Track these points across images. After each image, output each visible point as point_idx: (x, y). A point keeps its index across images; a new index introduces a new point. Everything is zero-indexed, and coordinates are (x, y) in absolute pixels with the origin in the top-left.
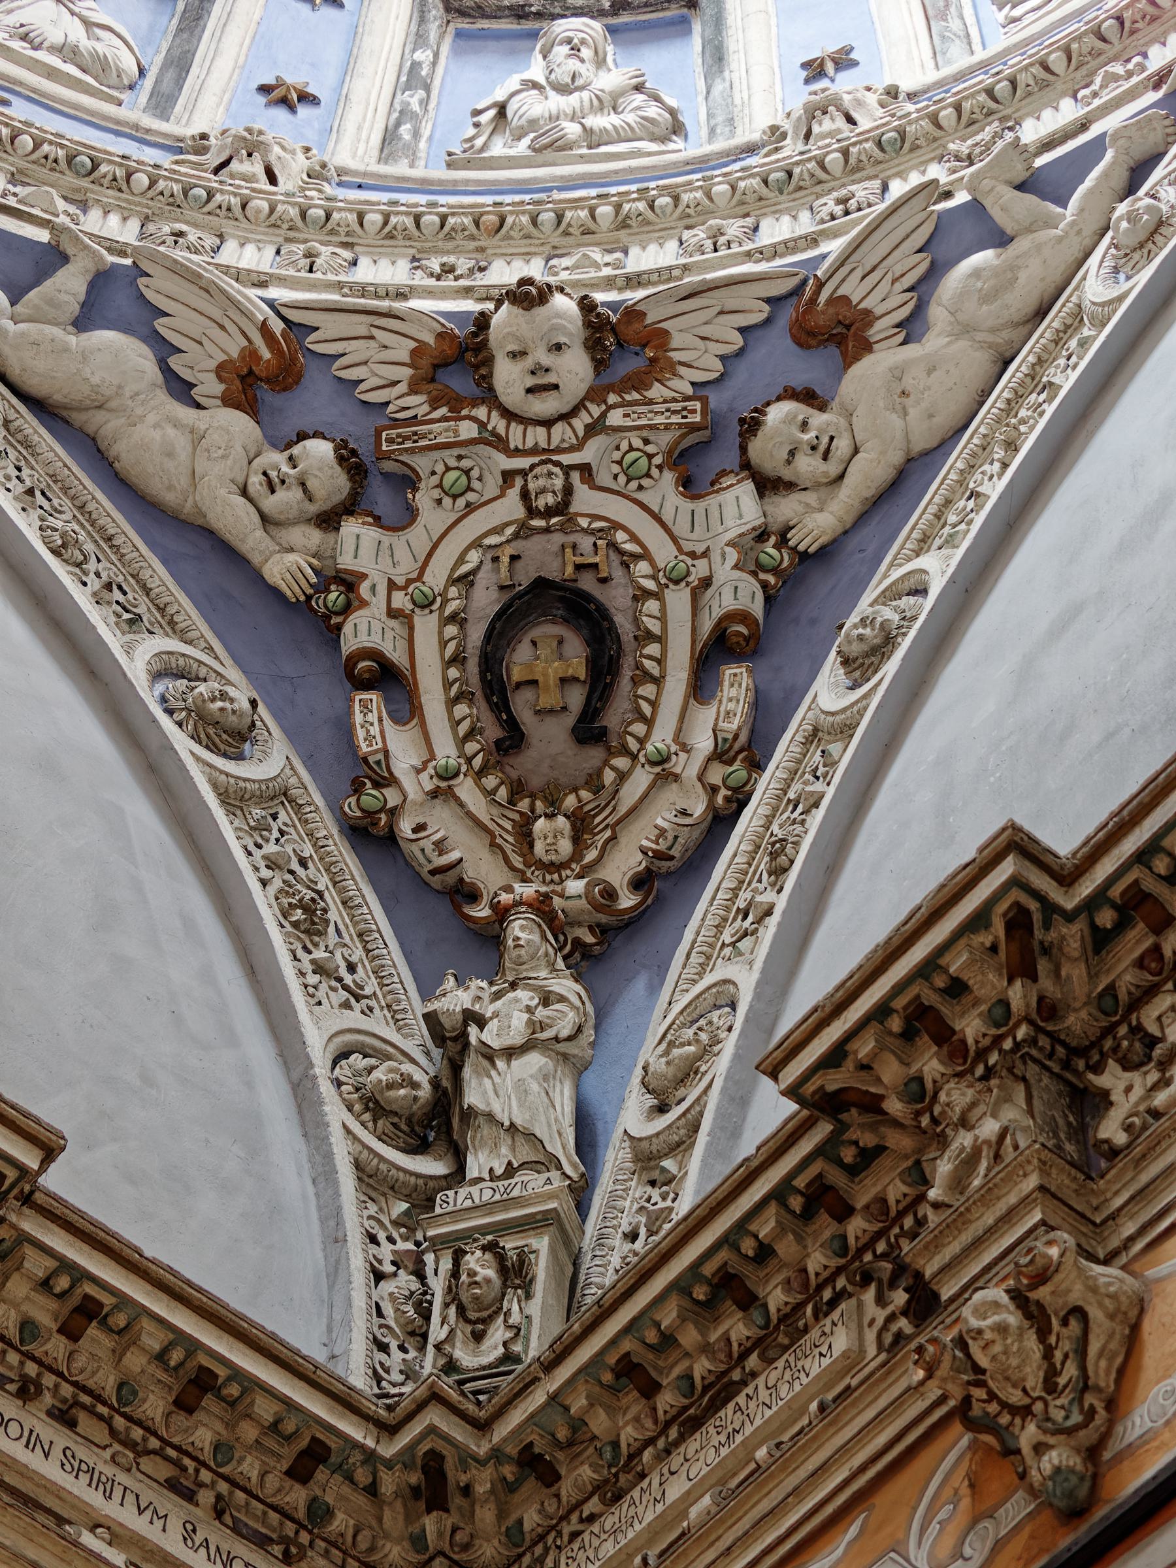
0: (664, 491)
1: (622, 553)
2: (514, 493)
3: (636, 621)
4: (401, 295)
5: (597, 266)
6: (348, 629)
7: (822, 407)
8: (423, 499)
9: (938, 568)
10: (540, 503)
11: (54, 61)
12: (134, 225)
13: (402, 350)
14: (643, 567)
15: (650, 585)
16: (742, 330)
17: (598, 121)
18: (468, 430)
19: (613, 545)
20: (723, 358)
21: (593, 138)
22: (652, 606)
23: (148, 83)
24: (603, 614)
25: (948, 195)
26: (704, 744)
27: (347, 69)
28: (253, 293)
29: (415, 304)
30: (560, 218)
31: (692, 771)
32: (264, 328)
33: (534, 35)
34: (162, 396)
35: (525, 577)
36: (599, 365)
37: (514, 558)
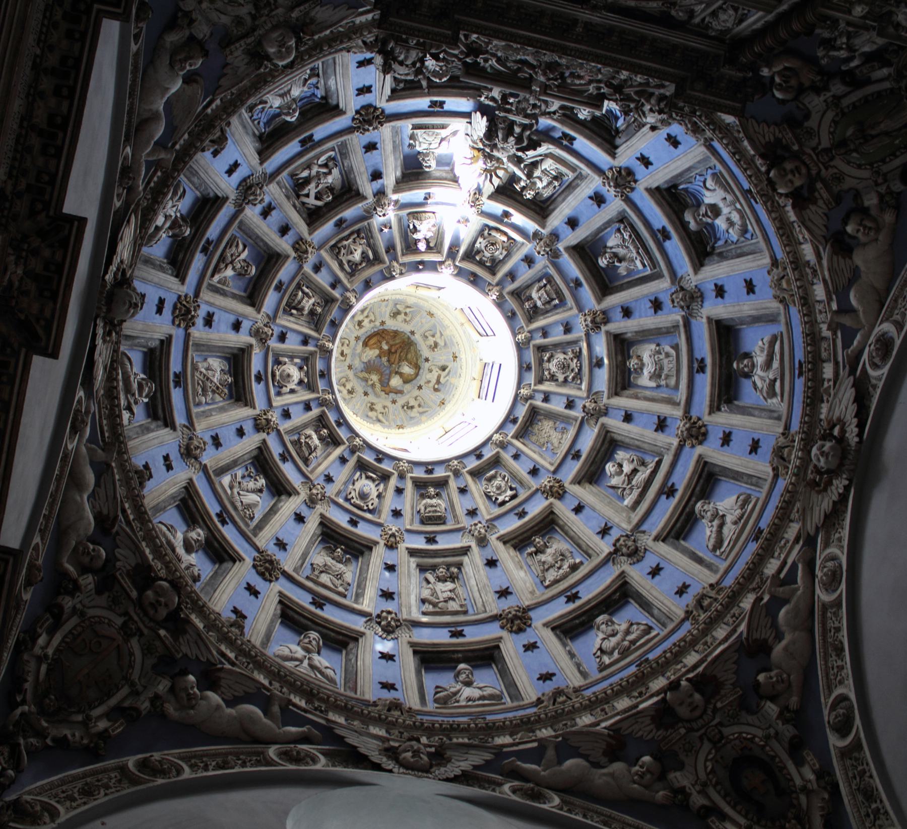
1: (748, 739)
4: (636, 706)
5: (680, 670)
6: (691, 803)
7: (770, 670)
9: (848, 690)
11: (481, 702)
13: (648, 720)
14: (757, 739)
15: (762, 743)
16: (734, 663)
17: (631, 637)
19: (745, 739)
20: (735, 673)
21: (633, 642)
22: (768, 748)
25: (762, 599)
26: (812, 777)
27: (555, 661)
28: (598, 728)
29: (642, 706)
30: (657, 663)
31: (815, 786)
32: (609, 735)
34: (595, 770)
36: (703, 695)
37: (722, 757)
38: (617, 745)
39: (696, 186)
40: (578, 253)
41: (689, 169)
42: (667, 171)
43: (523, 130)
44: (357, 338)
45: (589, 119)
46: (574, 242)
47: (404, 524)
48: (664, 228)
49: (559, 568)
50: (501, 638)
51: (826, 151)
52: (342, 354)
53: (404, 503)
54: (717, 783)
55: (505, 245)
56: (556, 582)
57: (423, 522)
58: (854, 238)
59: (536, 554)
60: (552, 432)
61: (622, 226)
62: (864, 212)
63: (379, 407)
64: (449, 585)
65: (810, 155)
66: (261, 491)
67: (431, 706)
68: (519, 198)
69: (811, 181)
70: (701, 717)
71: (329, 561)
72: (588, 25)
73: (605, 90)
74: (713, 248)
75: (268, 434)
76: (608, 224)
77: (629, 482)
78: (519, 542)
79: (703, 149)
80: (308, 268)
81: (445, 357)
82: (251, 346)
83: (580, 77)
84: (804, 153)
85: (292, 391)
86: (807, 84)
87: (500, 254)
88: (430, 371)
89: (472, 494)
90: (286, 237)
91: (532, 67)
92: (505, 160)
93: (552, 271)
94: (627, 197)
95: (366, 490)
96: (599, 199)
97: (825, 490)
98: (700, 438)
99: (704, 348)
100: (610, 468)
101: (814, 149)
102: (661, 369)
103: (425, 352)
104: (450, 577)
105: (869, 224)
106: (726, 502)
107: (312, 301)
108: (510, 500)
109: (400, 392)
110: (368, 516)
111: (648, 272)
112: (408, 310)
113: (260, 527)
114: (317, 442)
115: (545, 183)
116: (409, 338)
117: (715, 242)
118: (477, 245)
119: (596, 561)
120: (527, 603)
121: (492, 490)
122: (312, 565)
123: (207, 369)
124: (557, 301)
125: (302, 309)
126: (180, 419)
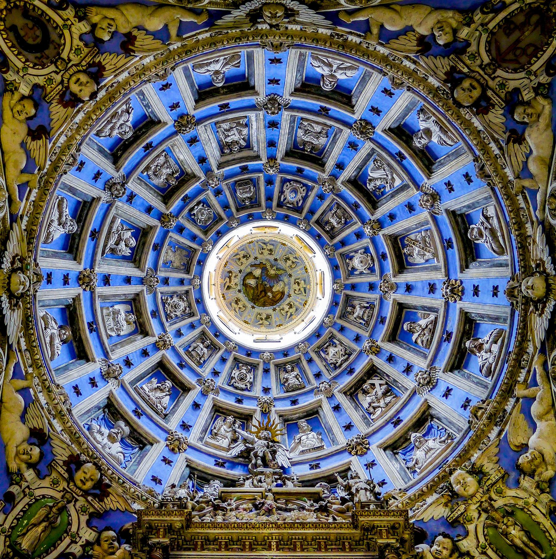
0: (41, 81)
1: (38, 65)
2: (66, 58)
3: (23, 56)
8: (81, 44)
10: (60, 61)
12: (172, 49)
14: (31, 65)
15: (27, 63)
18: (84, 63)
21: (109, 122)
22: (23, 60)
23: (191, 70)
24: (31, 52)
33: (134, 127)
35: (51, 46)
38: (127, 44)
39: (129, 451)
40: (186, 387)
41: (139, 463)
42: (152, 458)
43: (256, 463)
44: (289, 296)
45: (211, 482)
46: (191, 393)
47: (265, 176)
48: (139, 418)
49: (157, 166)
50: (195, 109)
51: (69, 502)
52: (298, 284)
53: (266, 190)
54: (56, 28)
55: (233, 381)
56: (158, 156)
57: (251, 180)
58: (31, 444)
59: (173, 173)
60: (172, 259)
61: (164, 412)
62: (30, 465)
63: (266, 252)
64: (229, 140)
65: (79, 496)
66: (370, 180)
67: (244, 52)
68: (235, 415)
69: (71, 479)
70: (71, 76)
71: (315, 142)
72: (269, 548)
73: (224, 505)
74: (104, 412)
75: (370, 220)
76: (173, 411)
77: (120, 235)
79: (138, 480)
80: (365, 334)
81: (229, 295)
82: (394, 276)
83: (245, 510)
84: (82, 496)
85: (356, 252)
87: (236, 373)
88: (236, 284)
90: (388, 355)
91: (279, 509)
92: (256, 439)
94: (168, 433)
95: (293, 195)
96: (185, 427)
97: (14, 258)
98: (82, 276)
99: (91, 340)
100: (133, 242)
101: (77, 500)
102: (114, 319)
103: (241, 296)
104: (229, 146)
106: (58, 233)
107: (355, 315)
108: (194, 207)
110: (289, 177)
111: (138, 384)
112: (261, 322)
113: (369, 155)
114: (332, 220)
115: (222, 429)
116: (255, 303)
117: (104, 416)
118: (252, 377)
119: (135, 176)
120: (178, 137)
122: (327, 137)
123: (424, 255)
124: (190, 349)
125: (361, 307)
126: (444, 218)
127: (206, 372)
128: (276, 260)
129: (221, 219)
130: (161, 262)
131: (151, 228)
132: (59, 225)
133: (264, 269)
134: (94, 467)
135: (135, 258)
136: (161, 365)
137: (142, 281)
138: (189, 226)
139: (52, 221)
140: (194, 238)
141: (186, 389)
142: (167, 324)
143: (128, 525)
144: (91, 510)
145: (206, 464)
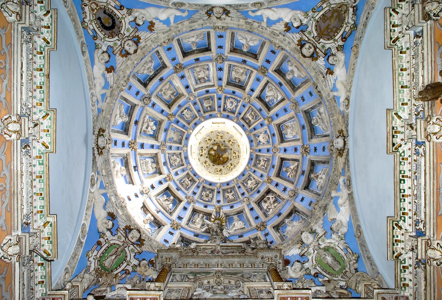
39: (153, 229)
41: (158, 234)
44: (231, 160)
60: (173, 137)
63: (219, 137)
69: (126, 237)
76: (174, 211)
78: (178, 96)
79: (158, 241)
86: (138, 268)
87: (204, 193)
88: (205, 154)
89: (196, 110)
93: (186, 192)
103: (208, 160)
105: (105, 225)
109: (213, 144)
119: (155, 94)
121: (189, 113)
127: (190, 193)
128: (224, 141)
129: (196, 117)
130: (168, 138)
131: (163, 121)
132: (120, 117)
133: (219, 146)
134: (137, 231)
135: (155, 136)
136: (168, 189)
137: (158, 148)
138: (181, 120)
139: (117, 115)
140: (184, 126)
141: (180, 201)
142: (171, 169)
143: (152, 259)
144: (136, 251)
145: (189, 235)
